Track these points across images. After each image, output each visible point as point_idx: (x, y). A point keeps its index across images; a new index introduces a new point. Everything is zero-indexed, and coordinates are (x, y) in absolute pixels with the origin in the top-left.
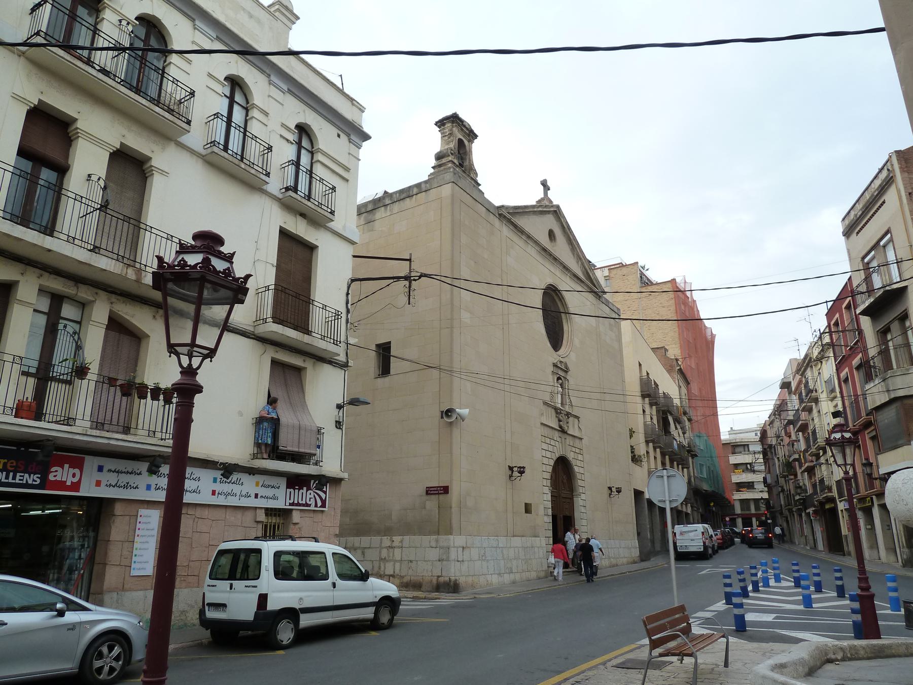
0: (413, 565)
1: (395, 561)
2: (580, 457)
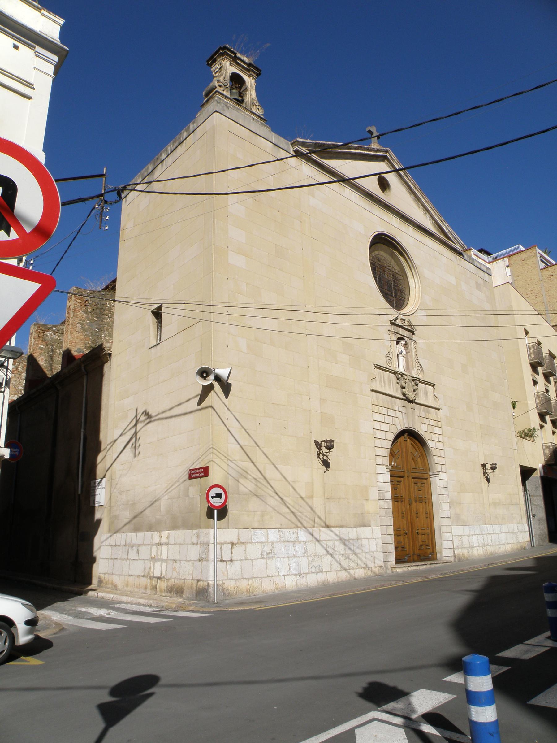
0: (177, 565)
1: (162, 561)
2: (437, 430)
